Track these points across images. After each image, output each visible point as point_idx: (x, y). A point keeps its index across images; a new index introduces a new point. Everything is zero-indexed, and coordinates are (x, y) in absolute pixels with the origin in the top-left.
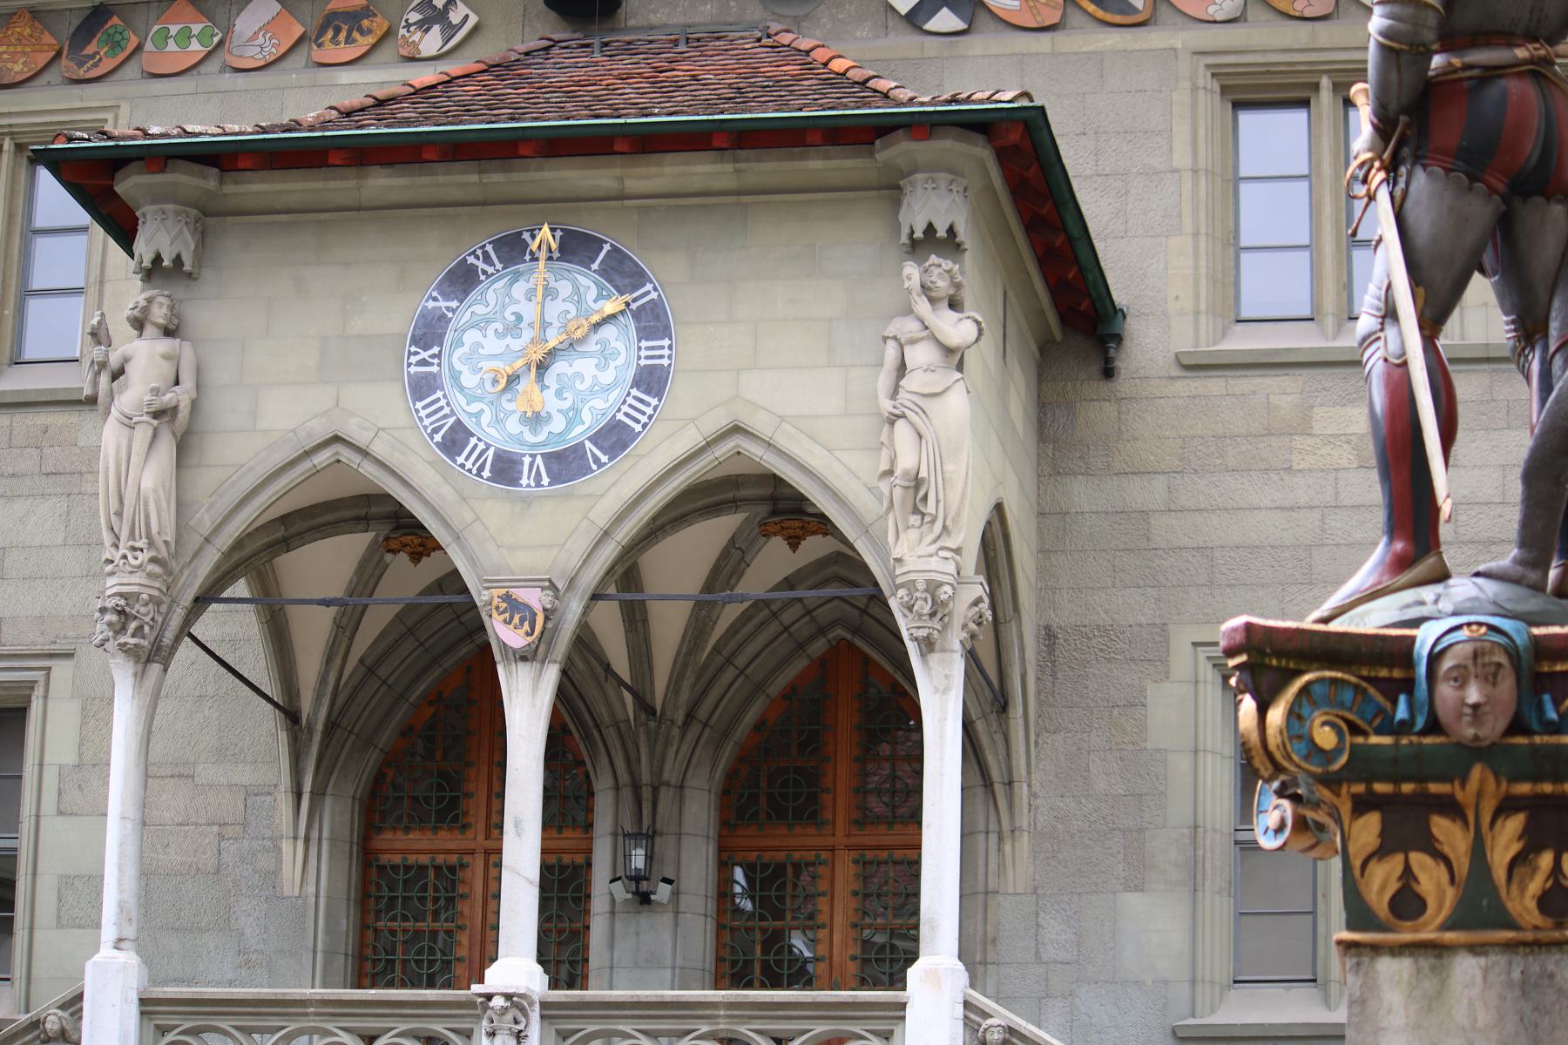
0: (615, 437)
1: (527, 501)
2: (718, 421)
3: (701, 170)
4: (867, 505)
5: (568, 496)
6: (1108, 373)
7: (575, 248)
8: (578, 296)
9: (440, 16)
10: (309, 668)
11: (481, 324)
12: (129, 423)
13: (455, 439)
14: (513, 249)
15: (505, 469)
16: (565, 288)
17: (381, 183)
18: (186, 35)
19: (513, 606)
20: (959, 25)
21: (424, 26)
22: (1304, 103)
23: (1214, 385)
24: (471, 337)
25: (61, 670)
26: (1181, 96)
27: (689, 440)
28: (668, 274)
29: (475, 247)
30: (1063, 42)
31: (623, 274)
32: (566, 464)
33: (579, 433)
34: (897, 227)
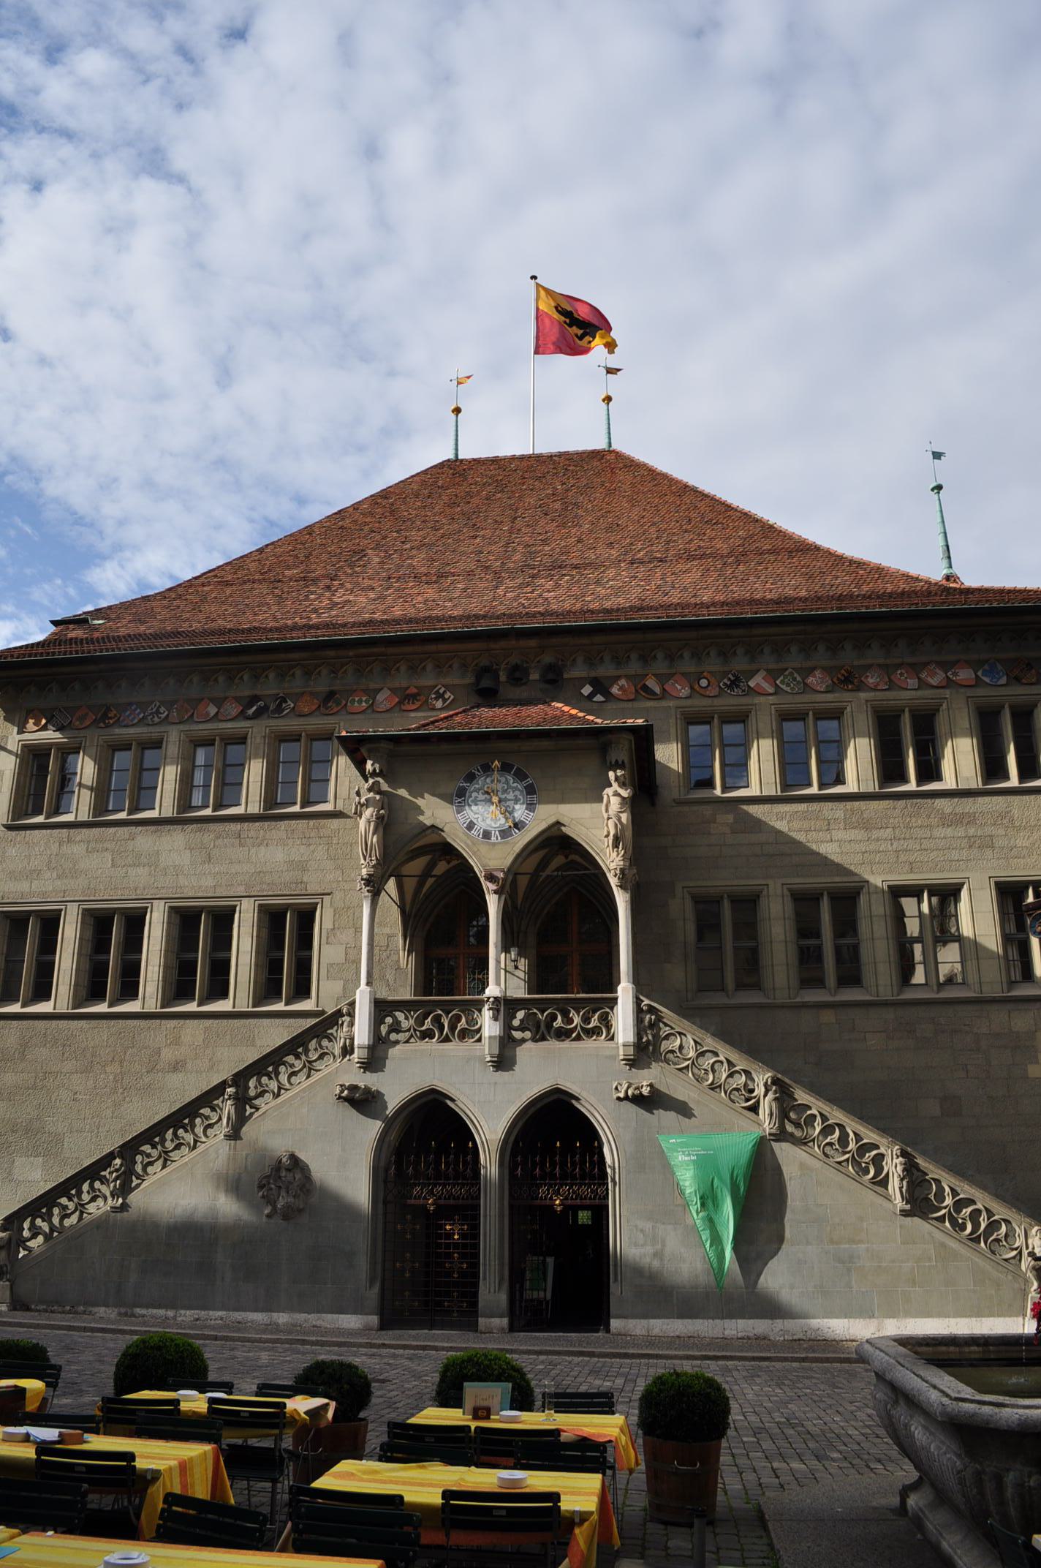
1: (494, 844)
2: (552, 820)
3: (545, 744)
5: (506, 843)
6: (653, 804)
7: (506, 768)
9: (440, 696)
10: (409, 897)
11: (477, 790)
13: (471, 826)
14: (487, 769)
15: (487, 835)
16: (503, 780)
17: (445, 747)
18: (360, 701)
20: (602, 699)
21: (437, 699)
22: (709, 723)
23: (686, 809)
24: (474, 794)
26: (672, 721)
30: (636, 704)
31: (520, 776)
34: (605, 761)
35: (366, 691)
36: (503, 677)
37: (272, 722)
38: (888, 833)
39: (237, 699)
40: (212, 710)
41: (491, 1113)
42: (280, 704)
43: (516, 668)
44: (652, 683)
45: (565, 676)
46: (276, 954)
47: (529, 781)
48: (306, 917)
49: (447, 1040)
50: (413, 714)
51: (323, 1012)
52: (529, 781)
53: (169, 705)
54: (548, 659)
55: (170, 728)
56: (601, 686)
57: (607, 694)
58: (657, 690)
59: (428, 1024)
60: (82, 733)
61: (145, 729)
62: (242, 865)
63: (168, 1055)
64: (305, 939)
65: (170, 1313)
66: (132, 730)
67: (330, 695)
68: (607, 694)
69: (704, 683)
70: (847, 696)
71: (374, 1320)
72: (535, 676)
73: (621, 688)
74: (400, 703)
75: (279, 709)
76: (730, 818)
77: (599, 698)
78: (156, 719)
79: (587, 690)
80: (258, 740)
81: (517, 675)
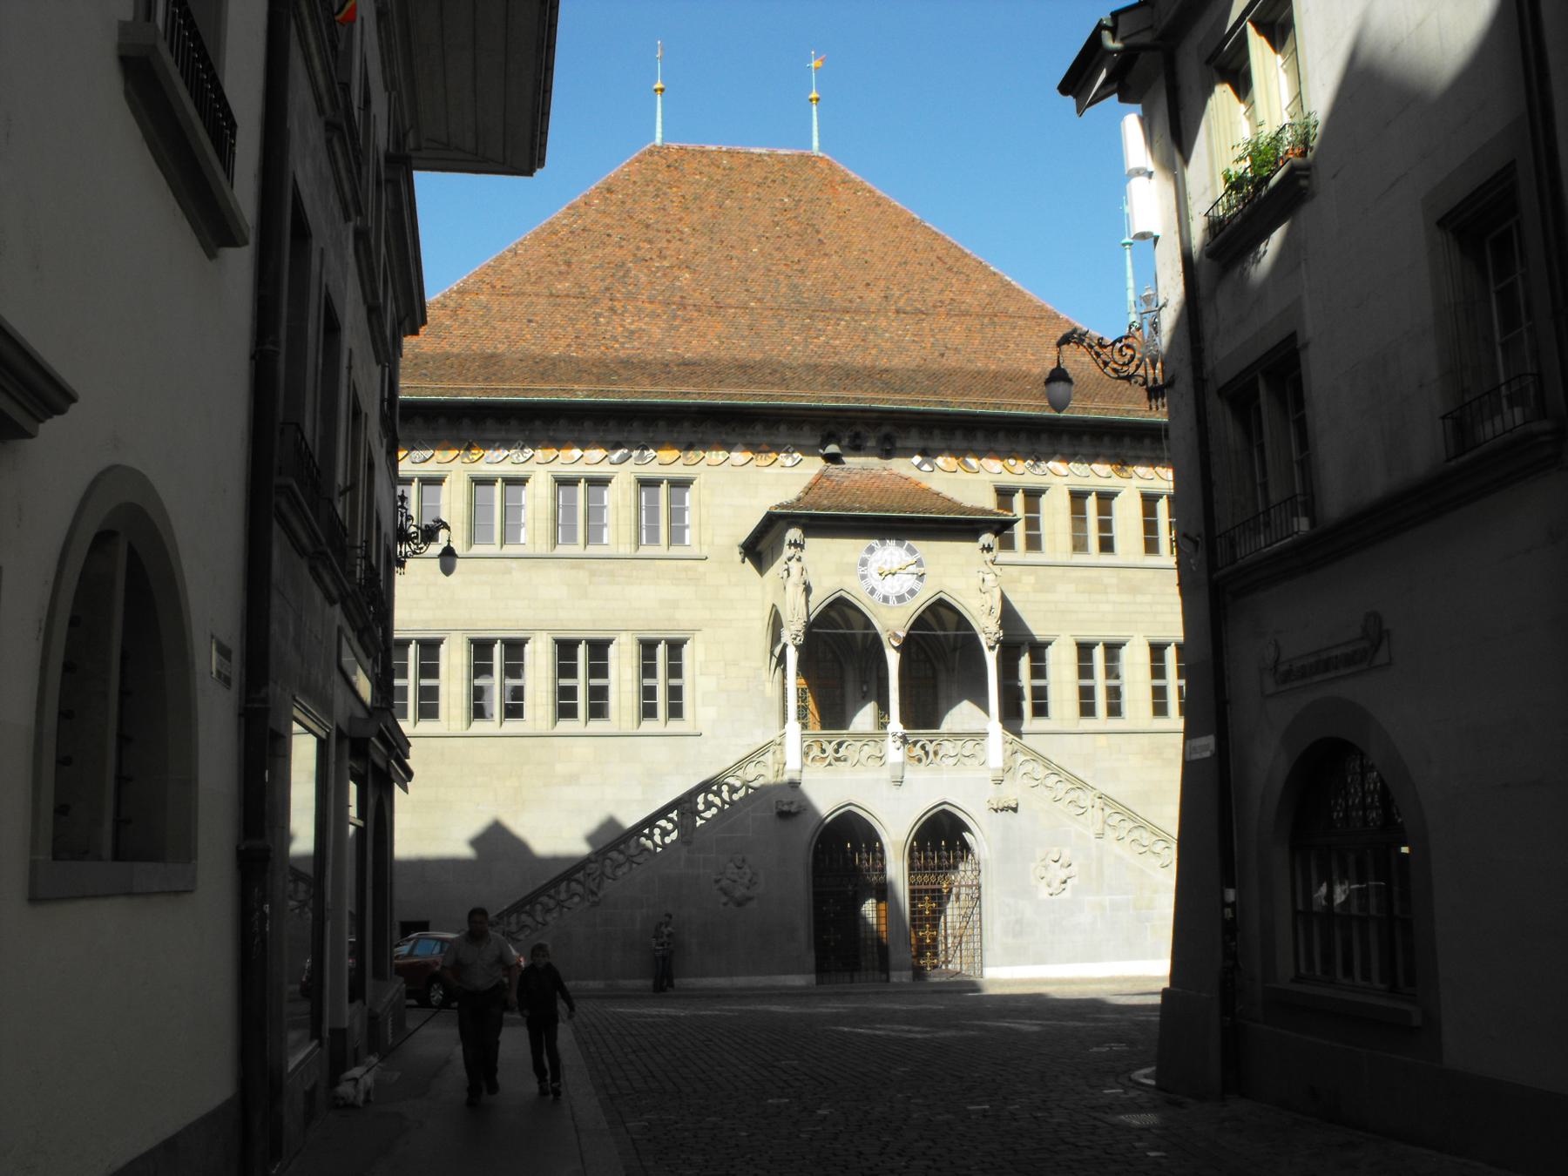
0: (912, 592)
12: (797, 585)
13: (872, 591)
15: (886, 599)
19: (895, 636)
25: (698, 635)
29: (874, 542)
32: (901, 599)
38: (1148, 598)
45: (898, 444)
46: (648, 682)
47: (918, 556)
48: (675, 647)
50: (767, 470)
52: (918, 556)
60: (447, 467)
62: (620, 600)
63: (560, 768)
64: (675, 670)
70: (1123, 482)
71: (812, 978)
72: (871, 443)
76: (1032, 579)
77: (926, 467)
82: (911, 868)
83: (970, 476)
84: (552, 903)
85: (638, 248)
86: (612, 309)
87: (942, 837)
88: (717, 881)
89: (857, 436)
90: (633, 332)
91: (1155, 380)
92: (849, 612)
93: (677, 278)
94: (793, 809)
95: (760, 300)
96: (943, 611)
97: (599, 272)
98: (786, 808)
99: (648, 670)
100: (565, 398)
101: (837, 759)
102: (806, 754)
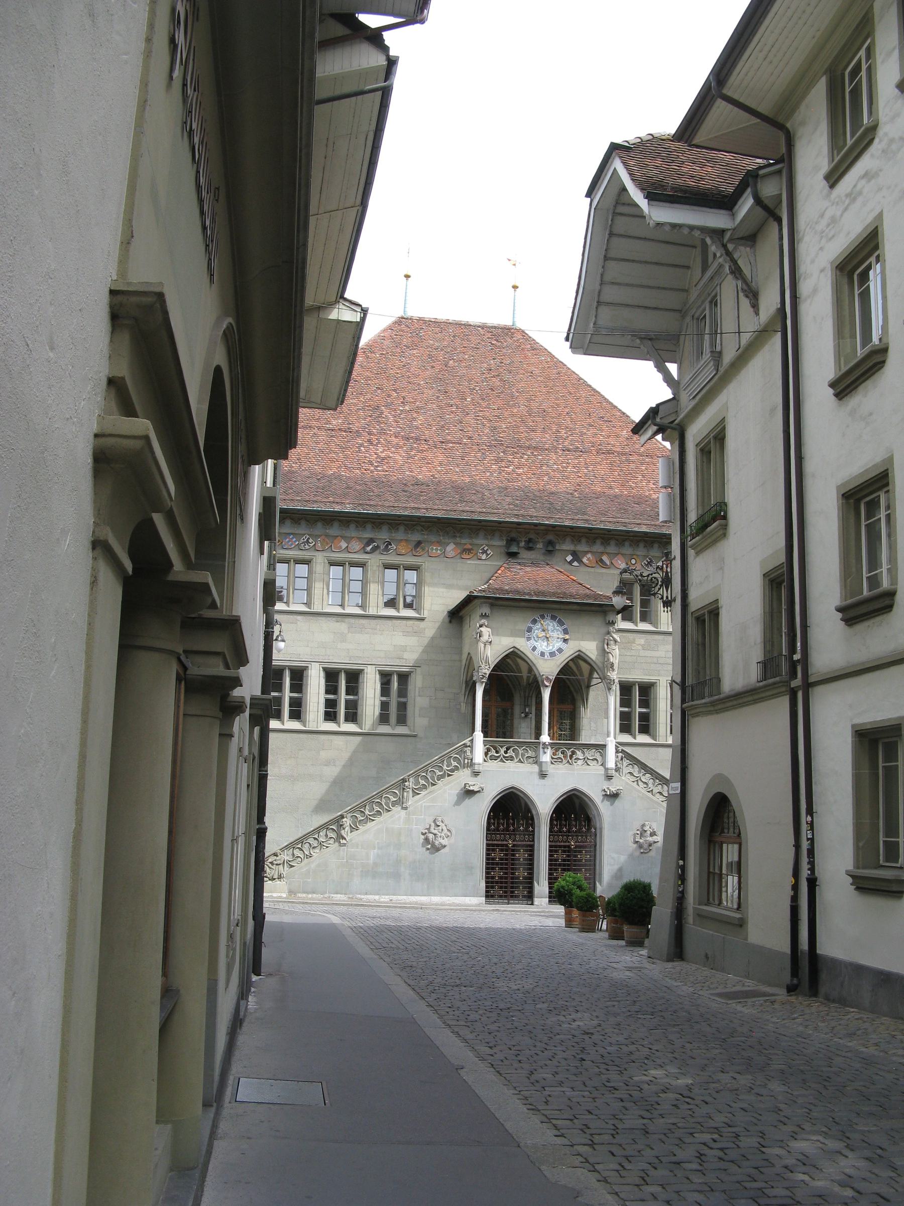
0: (560, 650)
3: (575, 607)
4: (600, 665)
7: (553, 618)
8: (554, 626)
9: (485, 552)
11: (538, 629)
13: (534, 649)
14: (543, 617)
15: (542, 654)
18: (437, 550)
19: (547, 679)
21: (483, 553)
27: (571, 653)
28: (568, 623)
31: (561, 623)
32: (552, 654)
33: (554, 649)
34: (605, 620)
35: (439, 543)
36: (522, 544)
37: (383, 557)
39: (359, 539)
40: (344, 545)
41: (544, 800)
42: (387, 546)
43: (530, 540)
44: (605, 558)
45: (557, 548)
48: (404, 678)
49: (520, 761)
51: (415, 736)
53: (315, 537)
54: (550, 537)
55: (317, 553)
56: (576, 557)
57: (580, 562)
58: (608, 563)
59: (511, 753)
61: (300, 553)
65: (377, 897)
66: (291, 552)
67: (419, 543)
68: (580, 562)
69: (633, 561)
72: (540, 546)
73: (588, 559)
74: (461, 553)
75: (386, 549)
76: (642, 641)
77: (575, 564)
78: (307, 546)
79: (569, 558)
80: (375, 568)
81: (531, 545)
82: (551, 831)
83: (604, 570)
84: (315, 843)
85: (389, 396)
86: (369, 441)
87: (573, 811)
88: (423, 834)
89: (530, 541)
90: (383, 459)
91: (667, 597)
92: (519, 661)
93: (414, 419)
94: (476, 789)
95: (470, 438)
96: (582, 663)
97: (361, 413)
98: (471, 788)
99: (385, 689)
100: (337, 508)
101: (507, 758)
102: (486, 754)
